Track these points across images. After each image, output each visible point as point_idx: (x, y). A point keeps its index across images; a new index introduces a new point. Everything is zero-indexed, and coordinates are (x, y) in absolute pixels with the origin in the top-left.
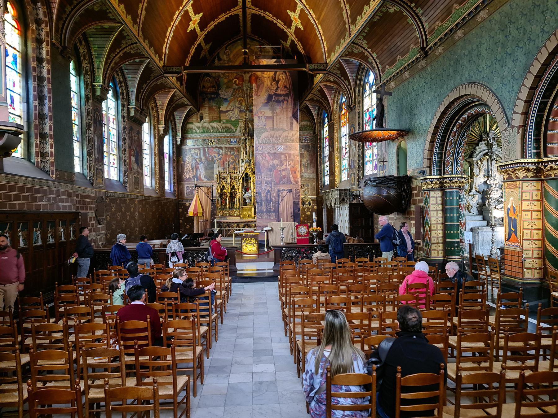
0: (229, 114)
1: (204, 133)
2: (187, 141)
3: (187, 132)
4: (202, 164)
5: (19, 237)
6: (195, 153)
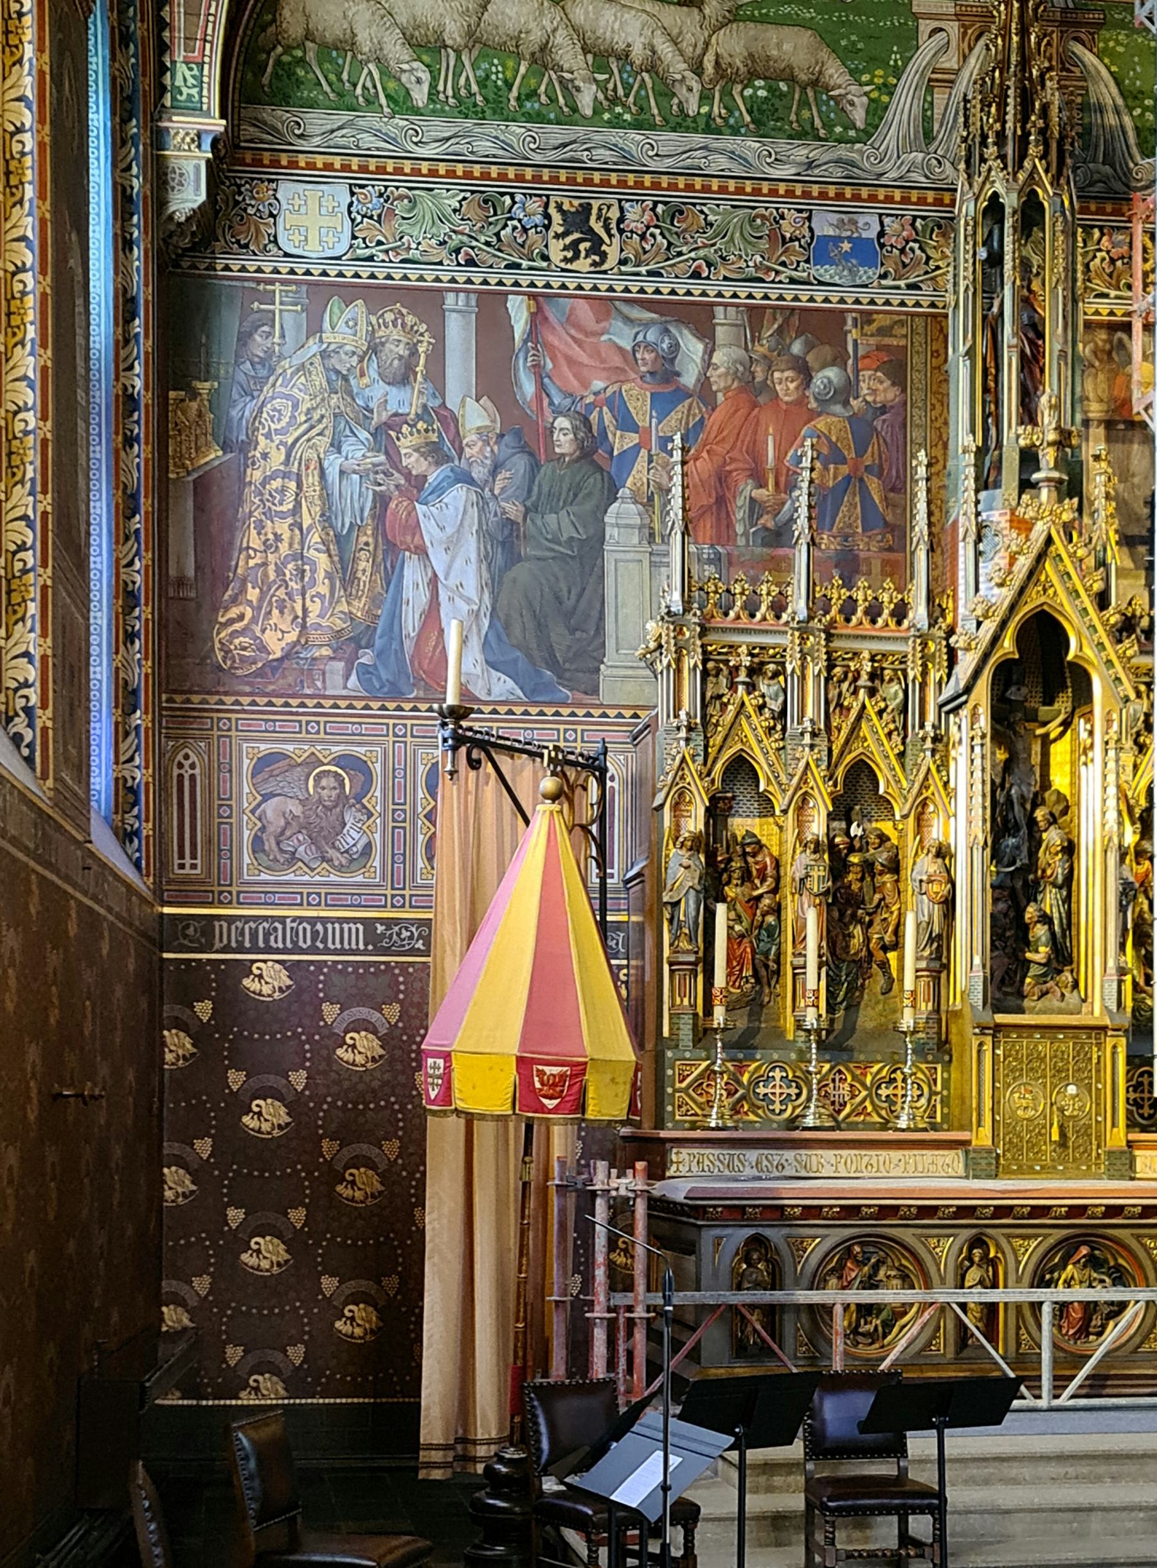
1: (496, 108)
2: (286, 190)
4: (458, 495)
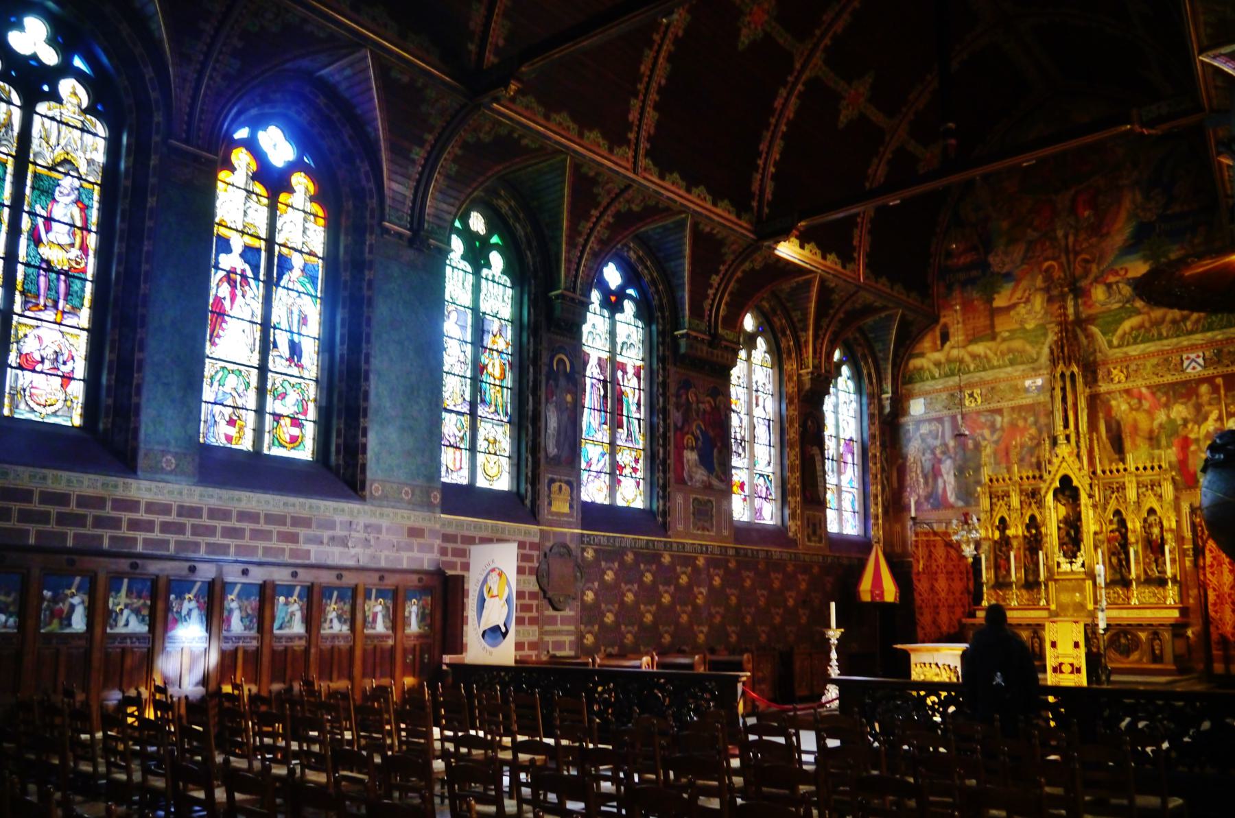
0: (1018, 314)
1: (952, 374)
2: (912, 402)
3: (910, 380)
5: (231, 611)
6: (930, 431)
